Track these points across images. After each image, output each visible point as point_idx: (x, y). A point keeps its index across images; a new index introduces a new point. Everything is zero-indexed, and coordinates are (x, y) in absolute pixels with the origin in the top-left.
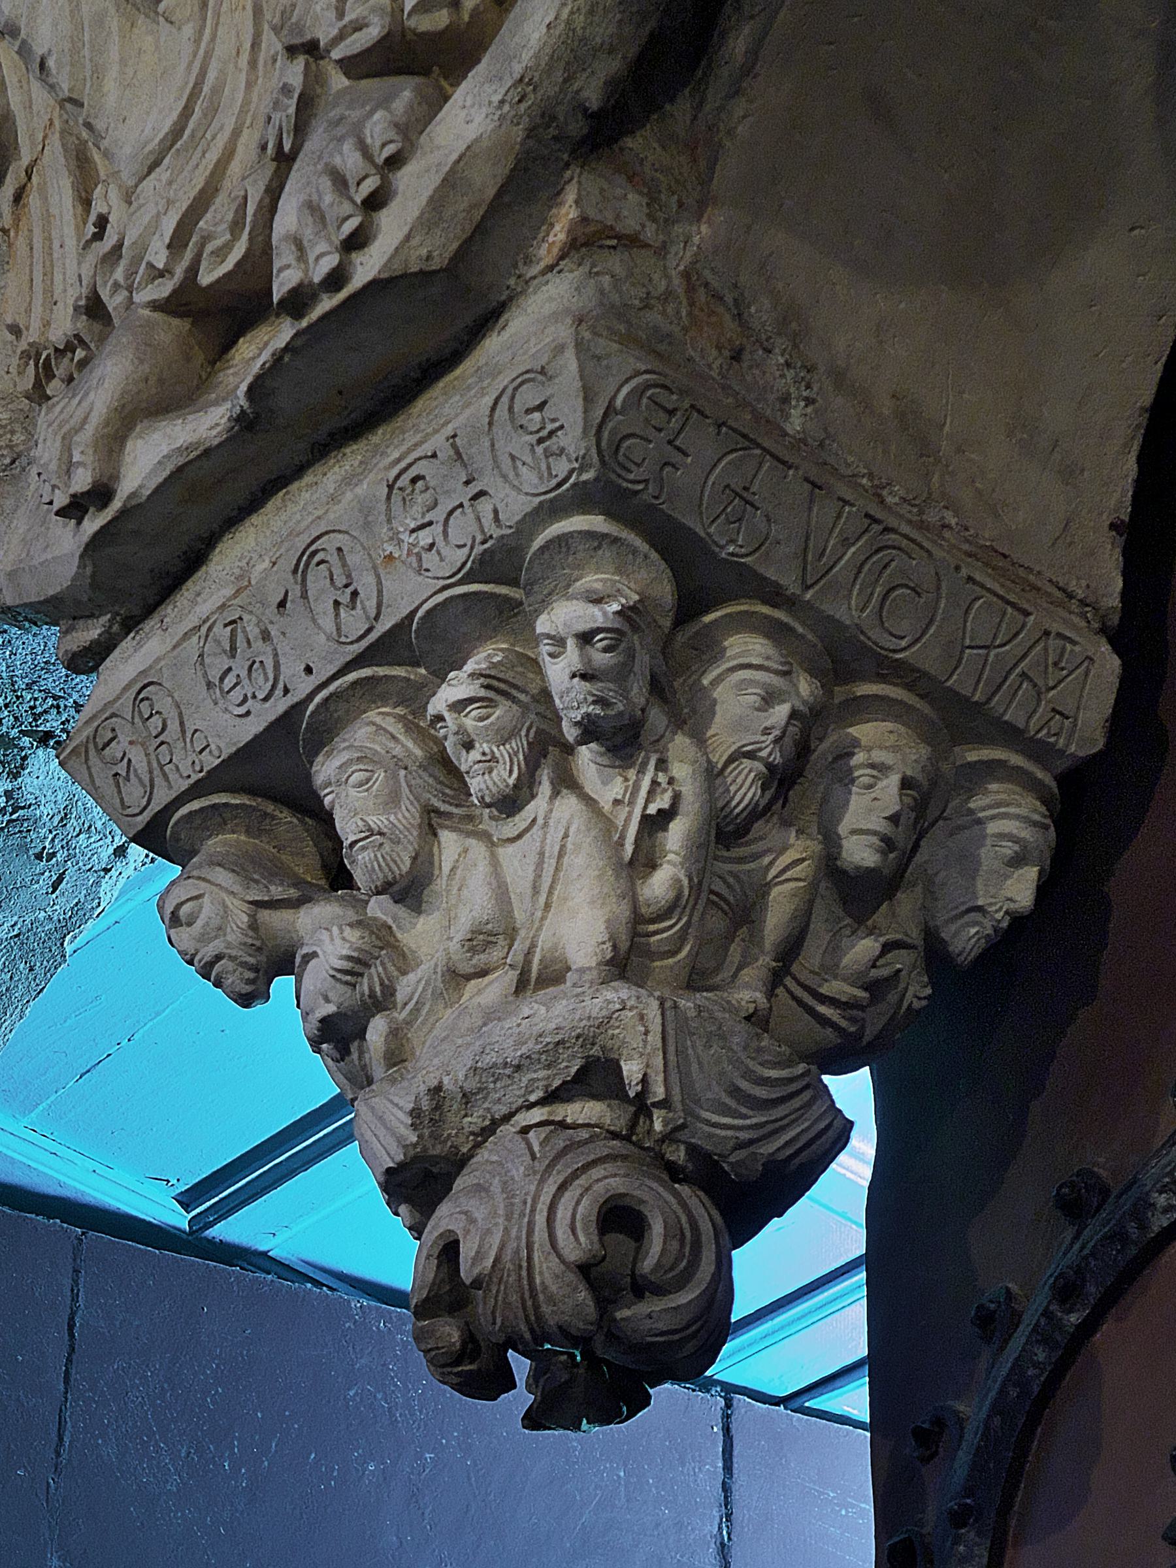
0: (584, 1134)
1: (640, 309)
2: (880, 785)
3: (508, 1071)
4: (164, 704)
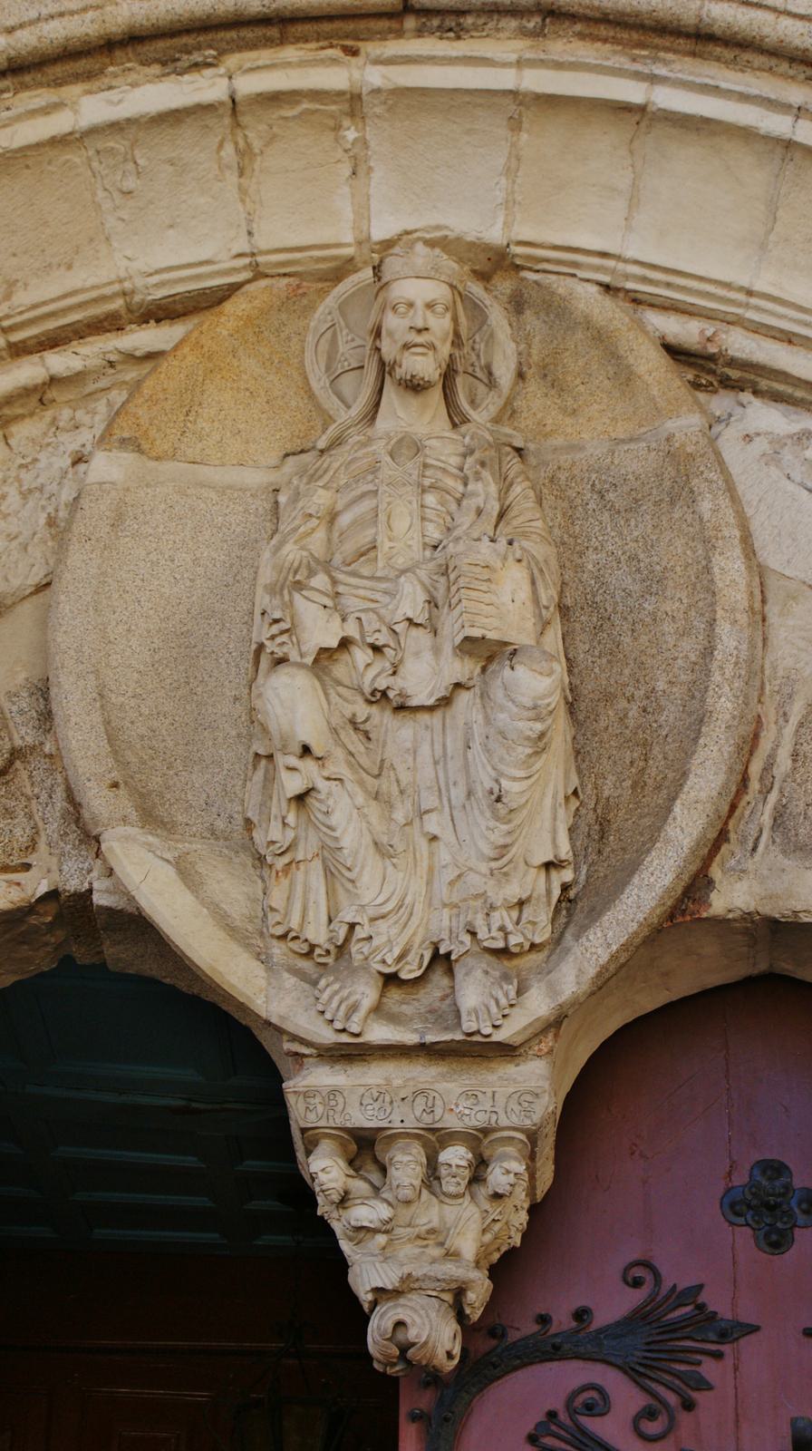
4: (341, 1100)
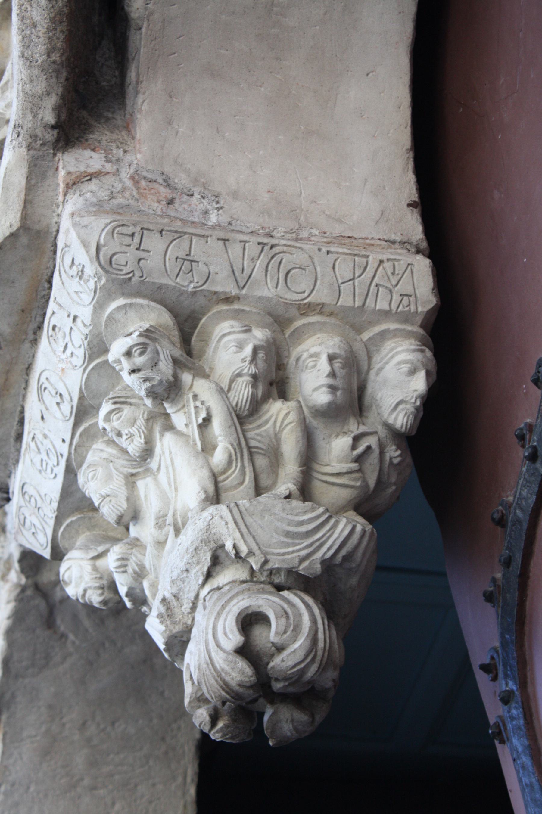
0: (227, 587)
1: (110, 200)
2: (319, 363)
3: (185, 575)
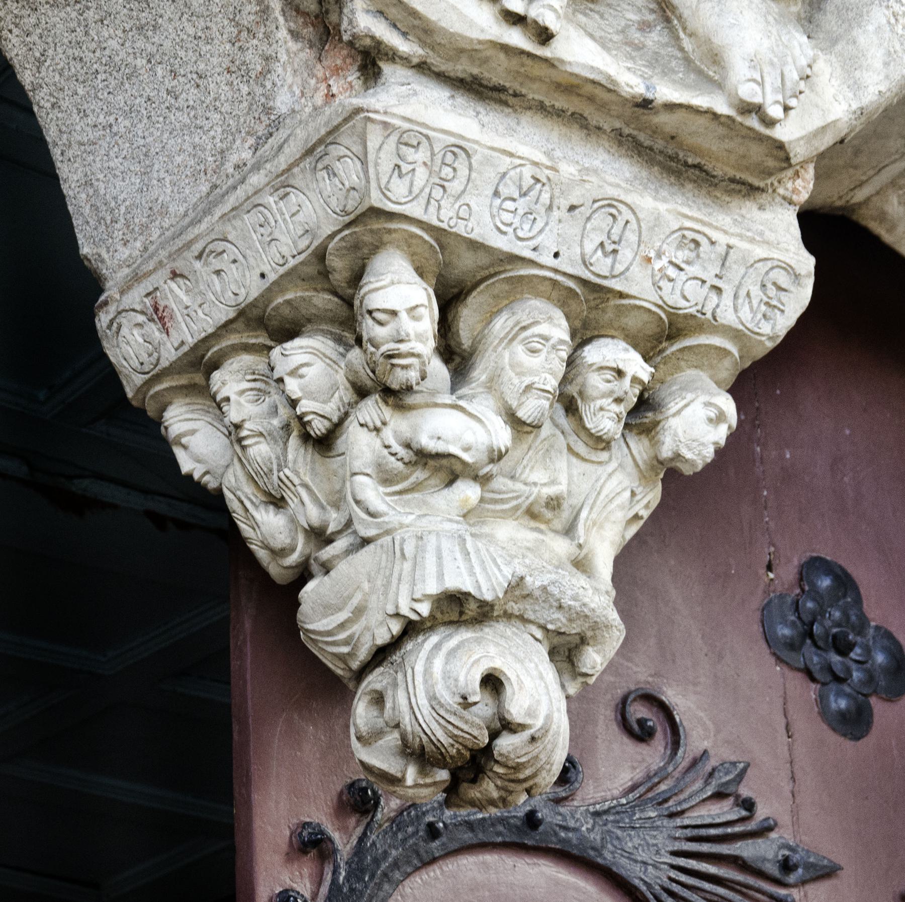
3: (555, 604)
4: (463, 171)
